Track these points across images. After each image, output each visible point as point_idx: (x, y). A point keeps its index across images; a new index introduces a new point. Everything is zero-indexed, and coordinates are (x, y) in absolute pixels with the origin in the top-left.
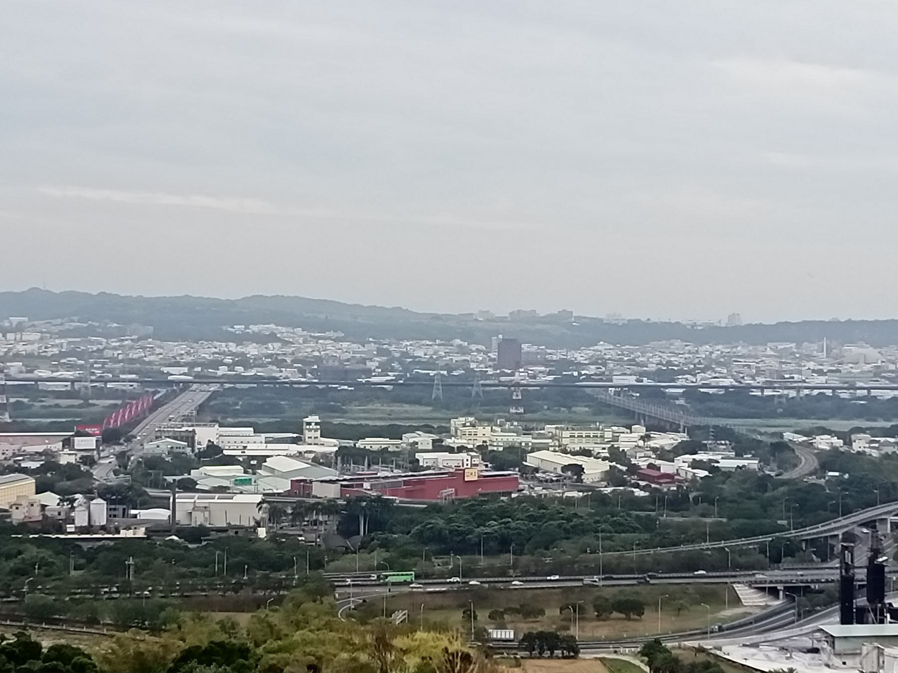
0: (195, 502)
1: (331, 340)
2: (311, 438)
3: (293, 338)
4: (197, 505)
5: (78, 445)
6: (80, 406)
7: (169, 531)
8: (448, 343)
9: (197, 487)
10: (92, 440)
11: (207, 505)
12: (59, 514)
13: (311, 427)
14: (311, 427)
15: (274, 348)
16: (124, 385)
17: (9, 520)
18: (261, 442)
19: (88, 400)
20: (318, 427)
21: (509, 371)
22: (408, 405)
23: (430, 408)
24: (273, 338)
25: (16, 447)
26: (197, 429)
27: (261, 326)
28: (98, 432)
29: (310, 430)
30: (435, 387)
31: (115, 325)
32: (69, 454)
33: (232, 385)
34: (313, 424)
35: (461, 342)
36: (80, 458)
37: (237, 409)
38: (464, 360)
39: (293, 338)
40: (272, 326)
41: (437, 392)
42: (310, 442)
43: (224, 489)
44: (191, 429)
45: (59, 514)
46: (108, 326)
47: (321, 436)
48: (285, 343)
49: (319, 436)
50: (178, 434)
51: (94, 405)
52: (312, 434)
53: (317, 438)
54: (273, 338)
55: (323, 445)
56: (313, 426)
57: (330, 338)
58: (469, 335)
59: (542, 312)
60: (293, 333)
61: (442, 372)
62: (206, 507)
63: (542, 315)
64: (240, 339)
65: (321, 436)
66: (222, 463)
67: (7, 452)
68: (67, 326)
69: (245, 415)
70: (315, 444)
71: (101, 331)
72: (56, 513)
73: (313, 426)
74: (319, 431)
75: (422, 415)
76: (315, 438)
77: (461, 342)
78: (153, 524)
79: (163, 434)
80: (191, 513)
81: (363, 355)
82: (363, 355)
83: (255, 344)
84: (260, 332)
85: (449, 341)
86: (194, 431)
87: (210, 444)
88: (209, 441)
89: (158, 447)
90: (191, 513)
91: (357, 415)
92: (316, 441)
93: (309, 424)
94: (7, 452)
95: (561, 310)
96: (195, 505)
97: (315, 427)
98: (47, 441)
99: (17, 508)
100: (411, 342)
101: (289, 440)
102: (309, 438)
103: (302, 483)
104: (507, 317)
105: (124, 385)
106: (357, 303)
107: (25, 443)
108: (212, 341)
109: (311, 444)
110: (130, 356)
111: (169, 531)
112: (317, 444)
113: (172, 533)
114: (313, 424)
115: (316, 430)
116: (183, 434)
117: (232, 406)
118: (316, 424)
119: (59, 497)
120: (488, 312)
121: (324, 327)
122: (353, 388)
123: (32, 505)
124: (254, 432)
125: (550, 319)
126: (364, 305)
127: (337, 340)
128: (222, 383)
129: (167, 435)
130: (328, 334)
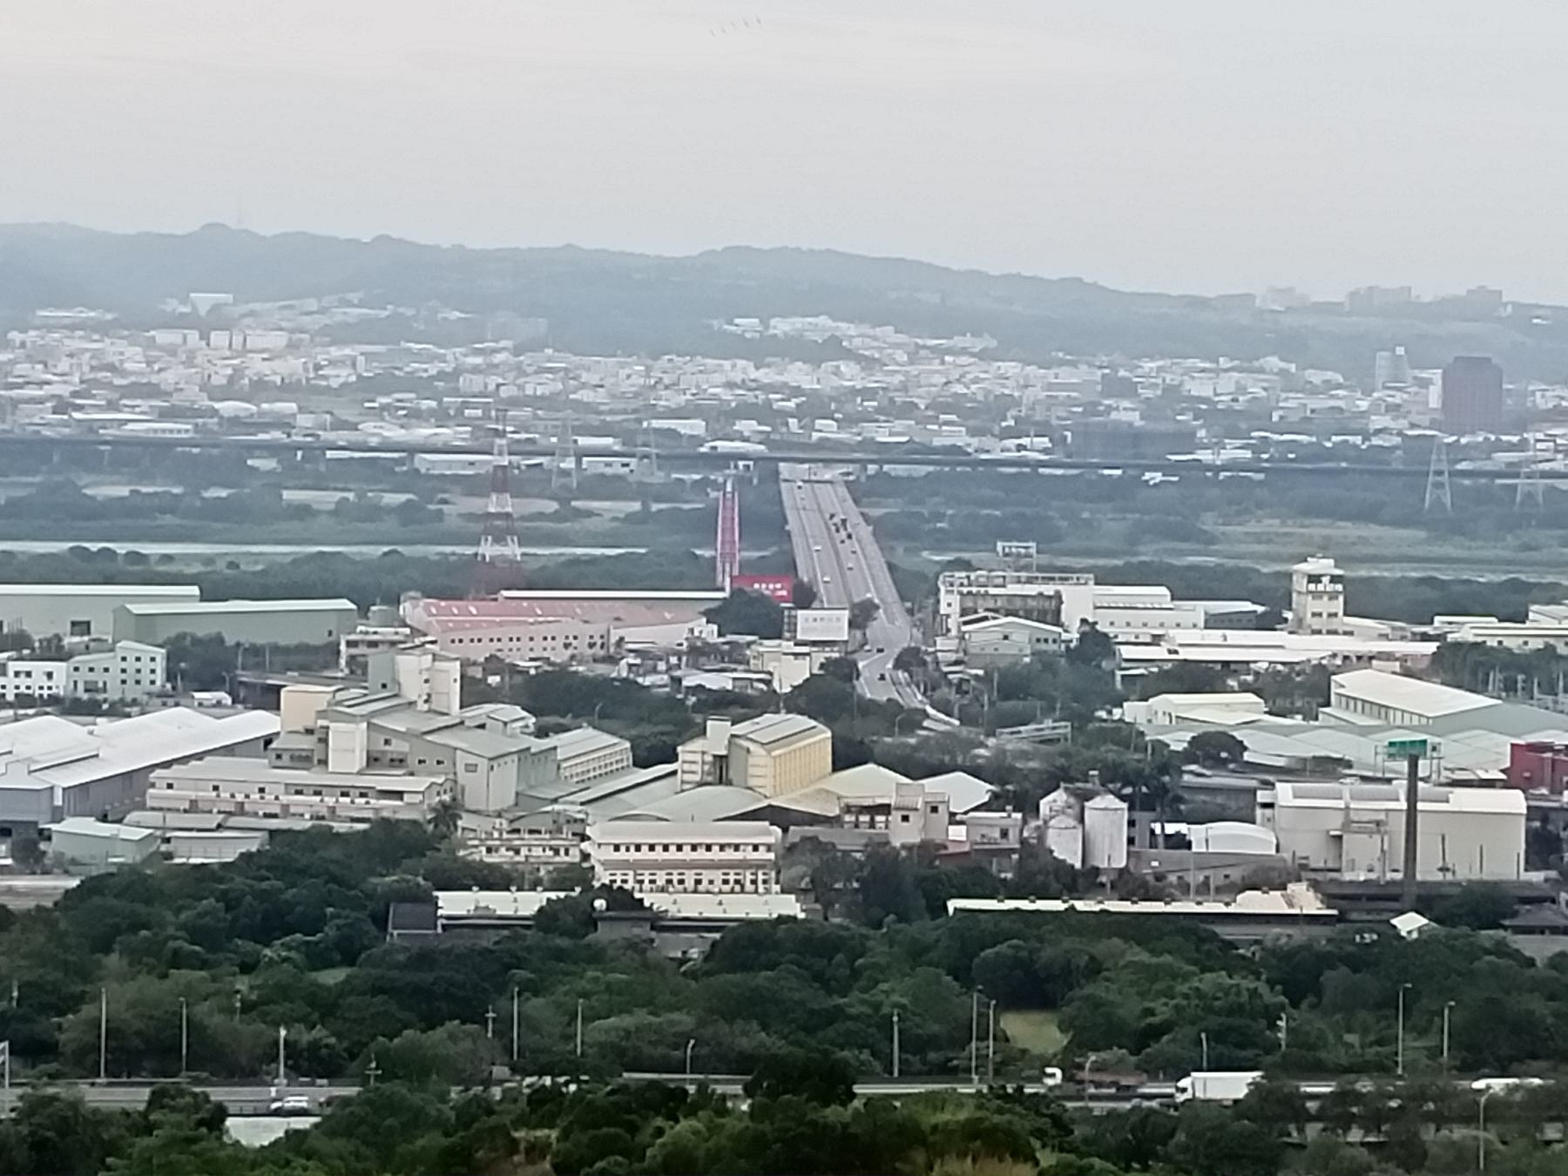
0: (1347, 808)
1: (973, 355)
2: (1320, 615)
3: (880, 349)
4: (1354, 816)
5: (803, 633)
6: (554, 517)
7: (1396, 898)
8: (1246, 365)
9: (1247, 756)
10: (838, 619)
11: (1382, 816)
12: (1004, 834)
13: (1320, 587)
14: (1320, 587)
15: (851, 375)
16: (608, 465)
17: (888, 848)
18: (1195, 626)
19: (569, 501)
20: (1339, 587)
21: (1515, 439)
22: (1349, 524)
23: (1422, 534)
24: (834, 349)
25: (596, 630)
26: (1065, 590)
27: (798, 322)
28: (784, 593)
29: (1317, 595)
30: (1431, 478)
31: (458, 314)
32: (796, 655)
33: (938, 468)
34: (1326, 580)
35: (1283, 365)
36: (822, 666)
37: (941, 529)
38: (1332, 408)
39: (880, 349)
40: (823, 320)
41: (1433, 496)
42: (1315, 627)
43: (1330, 767)
44: (1049, 590)
45: (1004, 834)
46: (440, 316)
47: (1346, 614)
48: (868, 363)
49: (1341, 613)
50: (1018, 603)
51: (589, 514)
52: (1324, 606)
53: (1336, 615)
54: (834, 349)
55: (1351, 633)
56: (1325, 585)
57: (964, 351)
58: (1293, 345)
59: (1426, 293)
60: (875, 338)
61: (1351, 439)
62: (1378, 823)
63: (1427, 298)
64: (760, 350)
65: (1346, 614)
66: (1186, 687)
67: (575, 643)
68: (339, 315)
69: (965, 545)
70: (1329, 632)
71: (422, 327)
72: (997, 834)
73: (1325, 585)
74: (1341, 598)
75: (1406, 550)
76: (1330, 615)
77: (1283, 365)
78: (1253, 866)
79: (980, 602)
80: (1340, 838)
81: (1074, 394)
82: (1074, 394)
83: (799, 364)
84: (802, 336)
85: (1251, 361)
86: (1058, 596)
87: (1086, 628)
88: (1084, 621)
89: (1006, 638)
90: (1340, 838)
91: (1243, 548)
92: (1334, 624)
93: (1314, 579)
94: (575, 643)
95: (1473, 287)
96: (1347, 815)
97: (1330, 588)
98: (668, 616)
99: (905, 818)
100: (1160, 363)
101: (1245, 618)
102: (1314, 615)
103: (1549, 755)
104: (1341, 304)
105: (608, 465)
106: (975, 267)
107: (618, 619)
108: (693, 355)
109: (1319, 632)
110: (529, 392)
111: (1396, 898)
112: (1335, 632)
113: (1407, 903)
114: (1326, 580)
115: (1333, 596)
116: (1032, 603)
117: (928, 521)
118: (1334, 579)
119: (989, 787)
120: (1290, 290)
121: (946, 322)
122: (1175, 479)
123: (935, 809)
124: (1173, 599)
125: (1445, 309)
126: (992, 273)
127: (984, 355)
128: (864, 463)
129: (991, 605)
130: (958, 341)
